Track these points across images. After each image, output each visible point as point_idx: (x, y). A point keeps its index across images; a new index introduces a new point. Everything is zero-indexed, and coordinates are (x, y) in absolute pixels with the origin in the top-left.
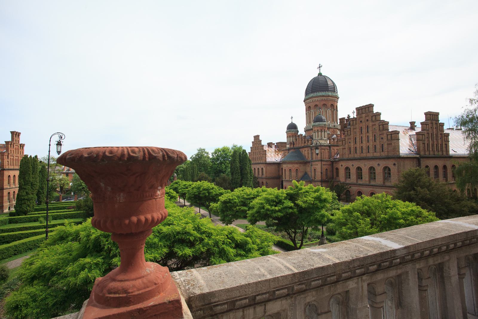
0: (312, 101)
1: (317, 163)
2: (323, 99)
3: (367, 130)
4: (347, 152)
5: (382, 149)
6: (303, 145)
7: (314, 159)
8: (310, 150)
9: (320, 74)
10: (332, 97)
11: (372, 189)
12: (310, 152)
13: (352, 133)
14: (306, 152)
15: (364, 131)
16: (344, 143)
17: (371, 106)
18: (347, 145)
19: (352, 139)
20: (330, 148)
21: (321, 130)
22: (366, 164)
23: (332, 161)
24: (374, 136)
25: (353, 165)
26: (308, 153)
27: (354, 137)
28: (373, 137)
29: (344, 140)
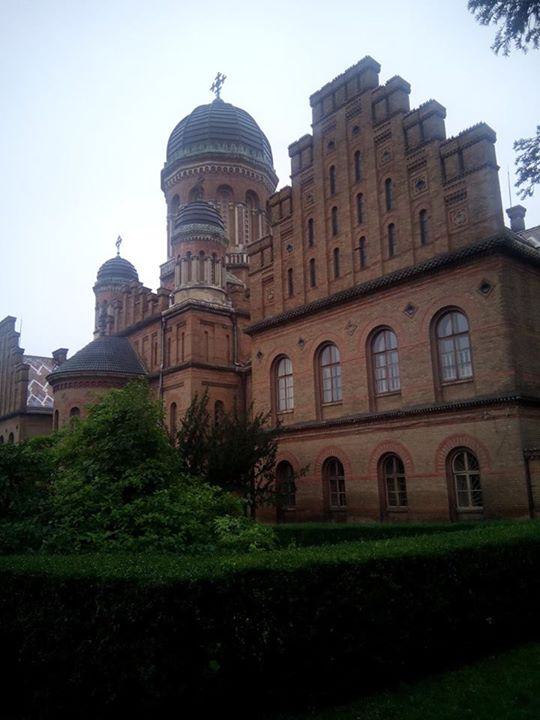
0: (185, 173)
1: (180, 376)
2: (219, 169)
3: (353, 173)
4: (278, 291)
5: (423, 235)
6: (139, 319)
7: (173, 365)
8: (160, 331)
9: (218, 103)
10: (249, 163)
11: (383, 436)
12: (159, 340)
13: (297, 203)
14: (148, 345)
15: (343, 177)
16: (267, 258)
17: (369, 67)
18: (278, 262)
19: (298, 230)
20: (235, 324)
21: (202, 253)
22: (353, 321)
23: (239, 374)
24: (383, 187)
25: (301, 341)
26: (155, 348)
27: (303, 222)
28: (380, 192)
29: (267, 242)
